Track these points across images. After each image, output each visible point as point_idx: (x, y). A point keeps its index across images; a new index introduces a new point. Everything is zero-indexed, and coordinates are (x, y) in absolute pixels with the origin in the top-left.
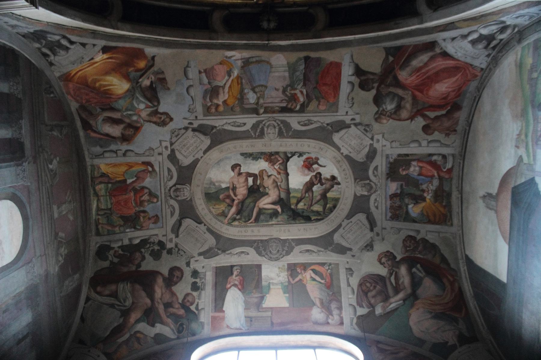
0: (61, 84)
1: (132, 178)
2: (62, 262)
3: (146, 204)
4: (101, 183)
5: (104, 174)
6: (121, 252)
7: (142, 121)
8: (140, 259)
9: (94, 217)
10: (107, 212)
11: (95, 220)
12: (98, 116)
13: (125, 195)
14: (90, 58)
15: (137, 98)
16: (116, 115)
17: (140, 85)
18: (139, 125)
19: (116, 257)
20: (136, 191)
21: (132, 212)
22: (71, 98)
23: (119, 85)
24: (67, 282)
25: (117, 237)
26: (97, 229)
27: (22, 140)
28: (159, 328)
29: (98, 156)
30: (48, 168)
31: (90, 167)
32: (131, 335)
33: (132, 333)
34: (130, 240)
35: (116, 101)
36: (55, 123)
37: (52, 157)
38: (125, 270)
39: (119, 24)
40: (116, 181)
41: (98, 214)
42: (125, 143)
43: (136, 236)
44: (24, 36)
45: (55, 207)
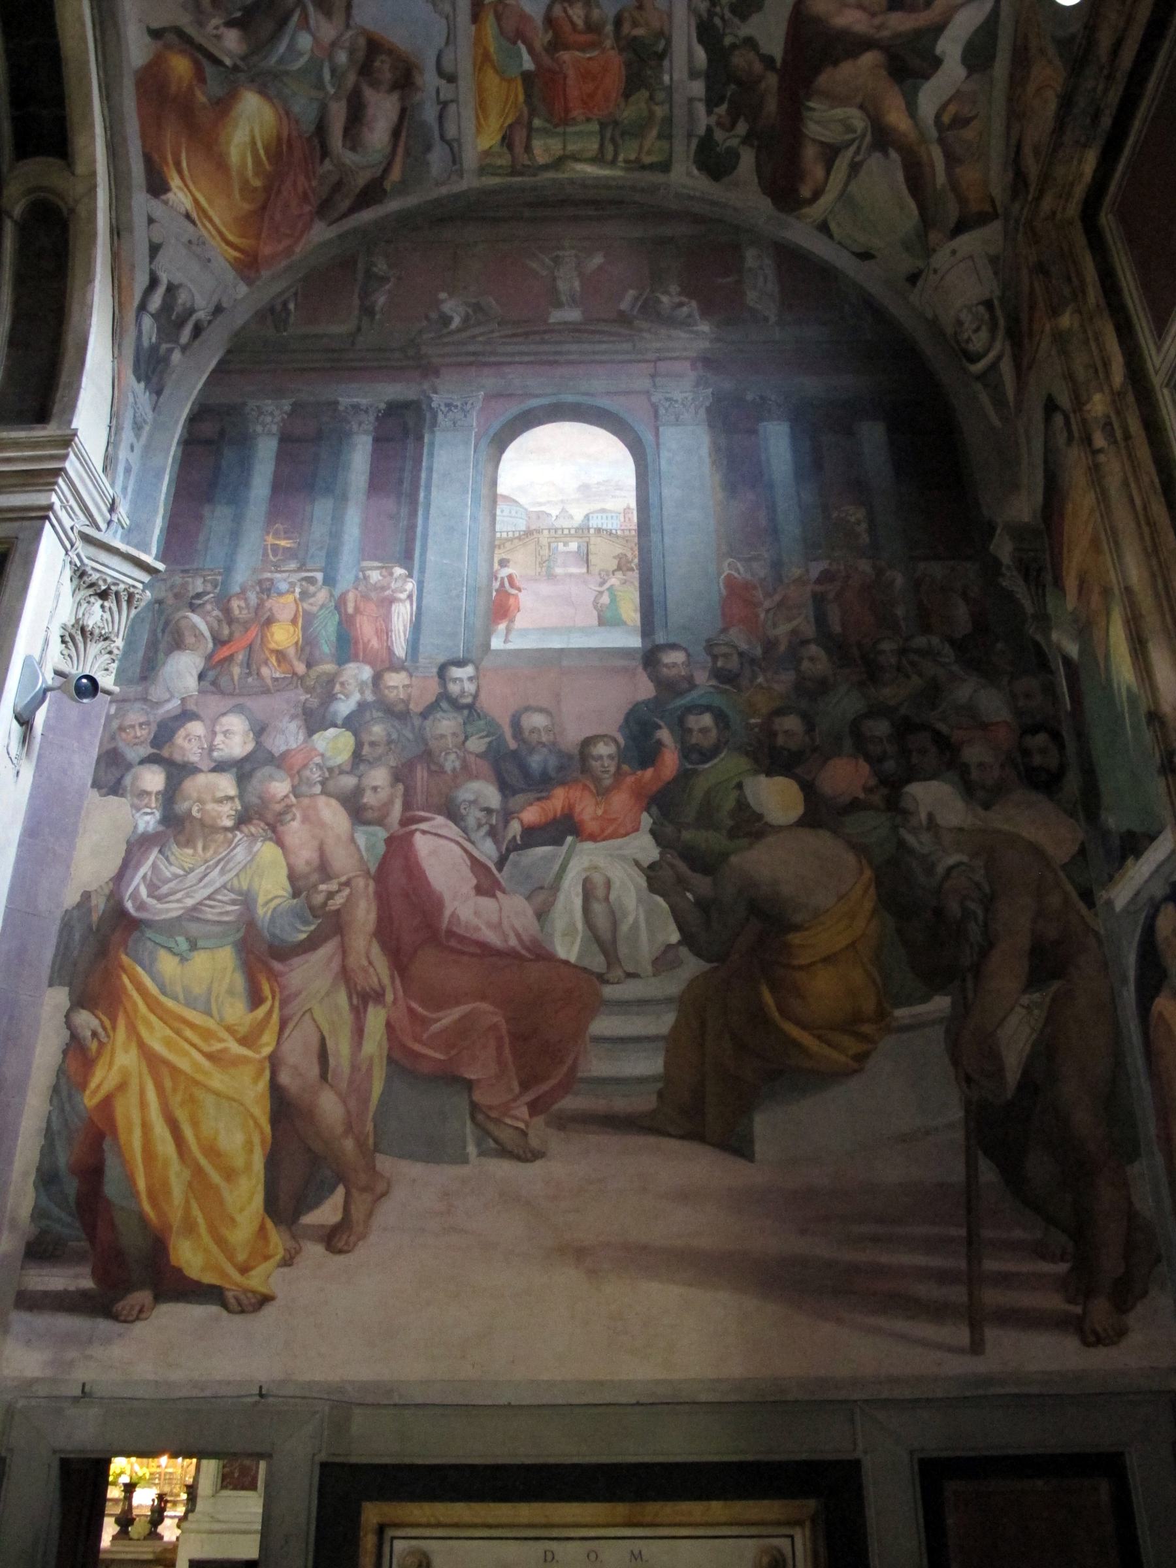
0: (265, 274)
1: (520, 56)
2: (694, 304)
3: (596, 13)
4: (528, 148)
5: (504, 138)
6: (722, 109)
7: (350, 33)
8: (752, 55)
9: (619, 173)
10: (608, 135)
11: (627, 169)
12: (344, 165)
13: (565, 77)
14: (187, 223)
15: (281, 60)
16: (338, 114)
17: (243, 58)
18: (362, 41)
19: (733, 125)
20: (556, 45)
21: (615, 61)
22: (303, 240)
23: (252, 121)
24: (751, 297)
25: (680, 114)
26: (651, 167)
27: (383, 406)
28: (951, 47)
29: (456, 159)
30: (459, 330)
31: (484, 179)
32: (941, 141)
33: (934, 133)
34: (693, 74)
35: (297, 122)
36: (356, 302)
37: (434, 315)
38: (771, 105)
39: (80, 169)
40: (525, 101)
41: (613, 163)
42: (419, 81)
43: (686, 54)
44: (159, 393)
45: (557, 316)
